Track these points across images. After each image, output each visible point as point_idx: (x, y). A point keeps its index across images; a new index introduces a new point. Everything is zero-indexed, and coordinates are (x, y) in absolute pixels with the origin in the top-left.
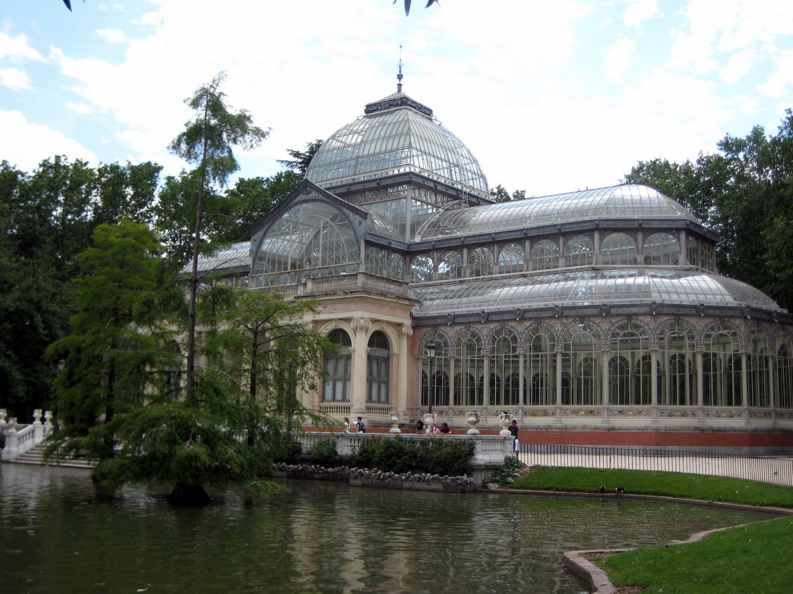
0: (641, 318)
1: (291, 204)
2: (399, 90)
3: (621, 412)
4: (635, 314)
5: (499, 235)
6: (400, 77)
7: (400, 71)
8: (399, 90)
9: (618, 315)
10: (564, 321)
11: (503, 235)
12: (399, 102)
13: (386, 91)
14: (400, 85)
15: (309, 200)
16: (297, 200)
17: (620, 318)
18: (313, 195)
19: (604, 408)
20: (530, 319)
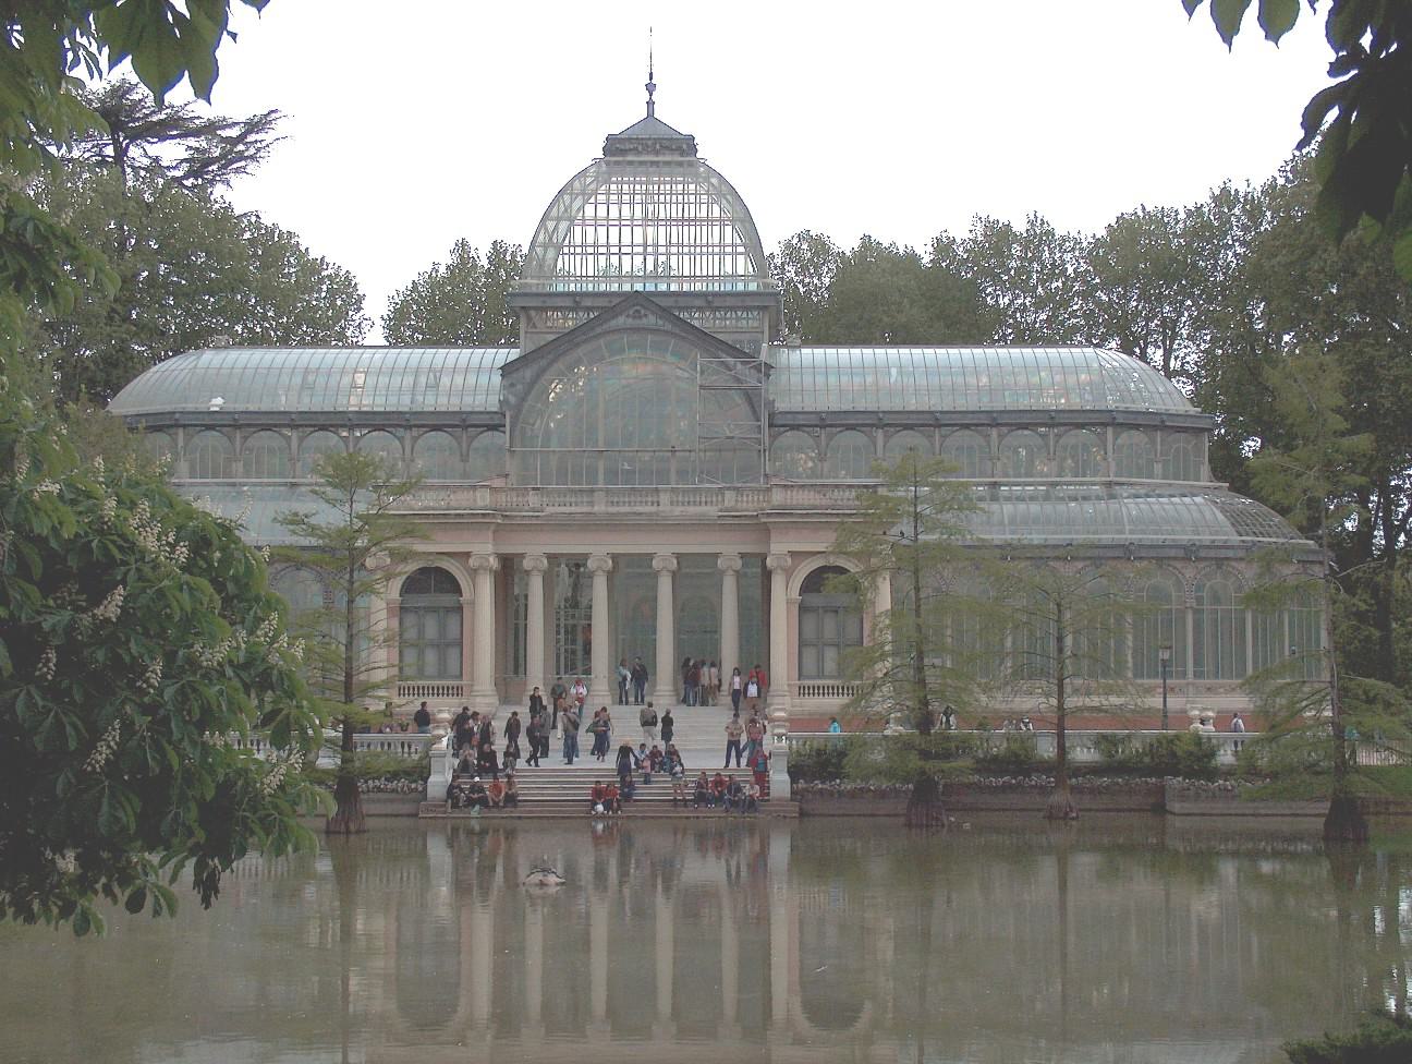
0: (1233, 563)
1: (598, 330)
2: (650, 113)
3: (1209, 689)
4: (1227, 559)
5: (948, 416)
6: (651, 88)
7: (651, 79)
8: (650, 113)
9: (1205, 559)
10: (1137, 563)
11: (954, 416)
12: (685, 147)
13: (626, 115)
14: (650, 104)
15: (644, 329)
16: (613, 323)
17: (1207, 563)
18: (651, 320)
19: (1188, 684)
20: (1084, 559)
